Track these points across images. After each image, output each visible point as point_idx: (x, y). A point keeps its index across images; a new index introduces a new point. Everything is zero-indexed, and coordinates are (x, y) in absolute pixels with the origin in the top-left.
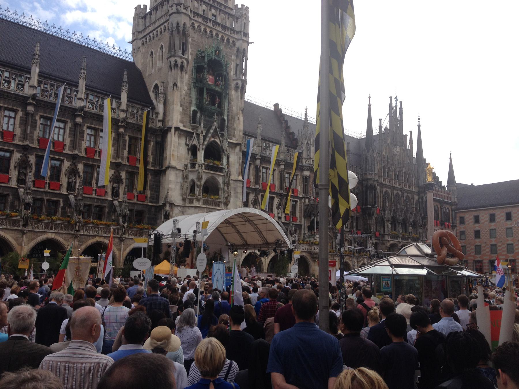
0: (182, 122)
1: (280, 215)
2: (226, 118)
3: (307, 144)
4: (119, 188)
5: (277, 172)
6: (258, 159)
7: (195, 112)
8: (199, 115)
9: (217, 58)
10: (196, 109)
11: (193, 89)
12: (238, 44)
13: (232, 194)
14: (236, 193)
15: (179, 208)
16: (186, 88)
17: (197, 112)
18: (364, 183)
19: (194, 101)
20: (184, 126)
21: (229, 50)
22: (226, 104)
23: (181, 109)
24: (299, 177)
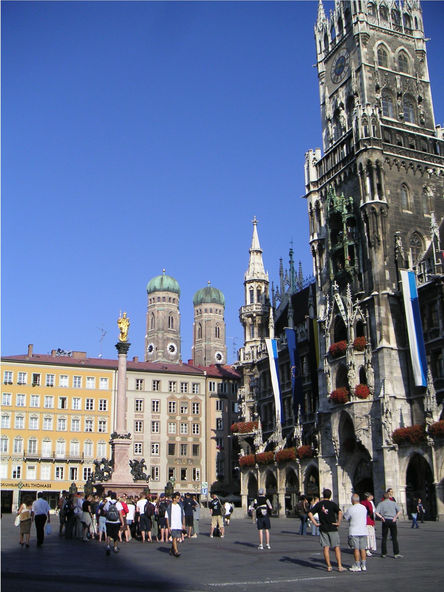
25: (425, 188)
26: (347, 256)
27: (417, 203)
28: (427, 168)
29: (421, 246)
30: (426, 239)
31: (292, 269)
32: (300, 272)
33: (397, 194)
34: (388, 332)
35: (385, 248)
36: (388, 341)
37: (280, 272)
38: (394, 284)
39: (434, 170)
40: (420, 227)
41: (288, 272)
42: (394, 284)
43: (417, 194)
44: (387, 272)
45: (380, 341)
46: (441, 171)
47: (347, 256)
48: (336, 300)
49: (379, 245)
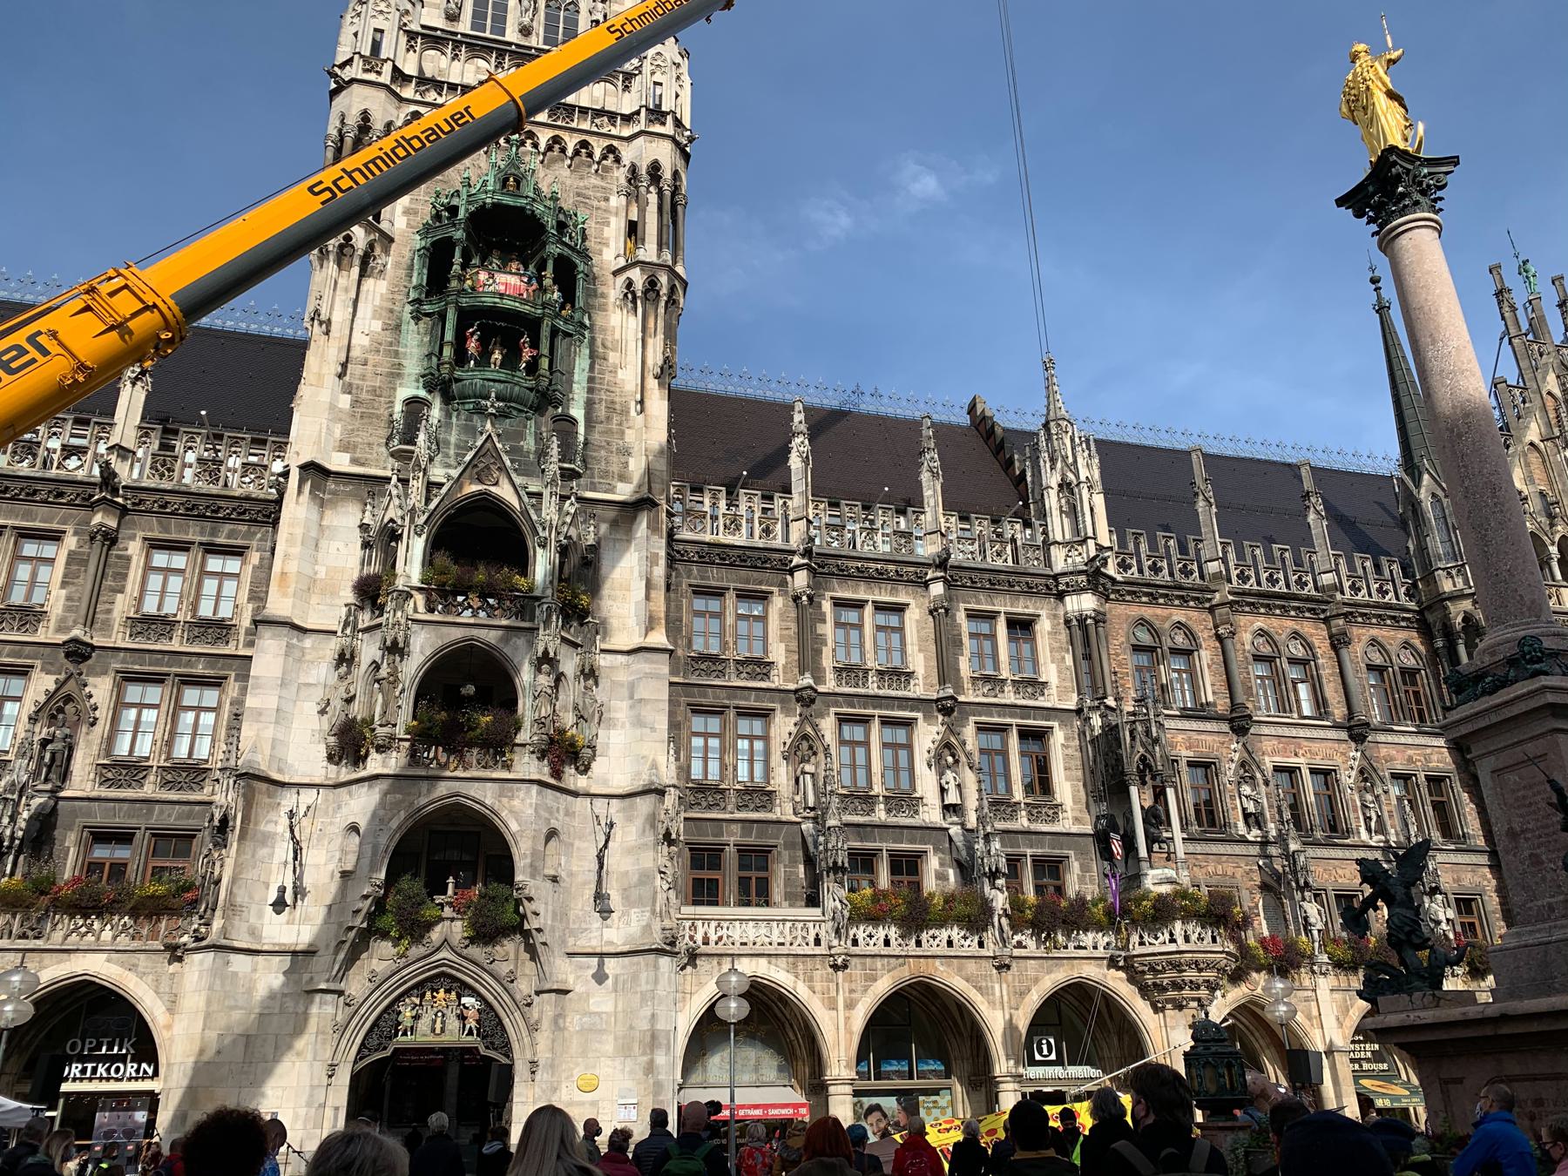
0: (345, 447)
1: (952, 798)
2: (577, 412)
3: (1065, 486)
4: (71, 749)
5: (915, 617)
6: (798, 567)
8: (436, 412)
10: (422, 393)
11: (410, 327)
12: (628, 153)
13: (620, 709)
14: (637, 703)
15: (308, 796)
16: (377, 326)
17: (428, 404)
18: (1430, 618)
19: (413, 366)
20: (354, 461)
21: (595, 181)
22: (581, 364)
23: (345, 401)
24: (1044, 626)
45: (649, 628)
48: (499, 446)
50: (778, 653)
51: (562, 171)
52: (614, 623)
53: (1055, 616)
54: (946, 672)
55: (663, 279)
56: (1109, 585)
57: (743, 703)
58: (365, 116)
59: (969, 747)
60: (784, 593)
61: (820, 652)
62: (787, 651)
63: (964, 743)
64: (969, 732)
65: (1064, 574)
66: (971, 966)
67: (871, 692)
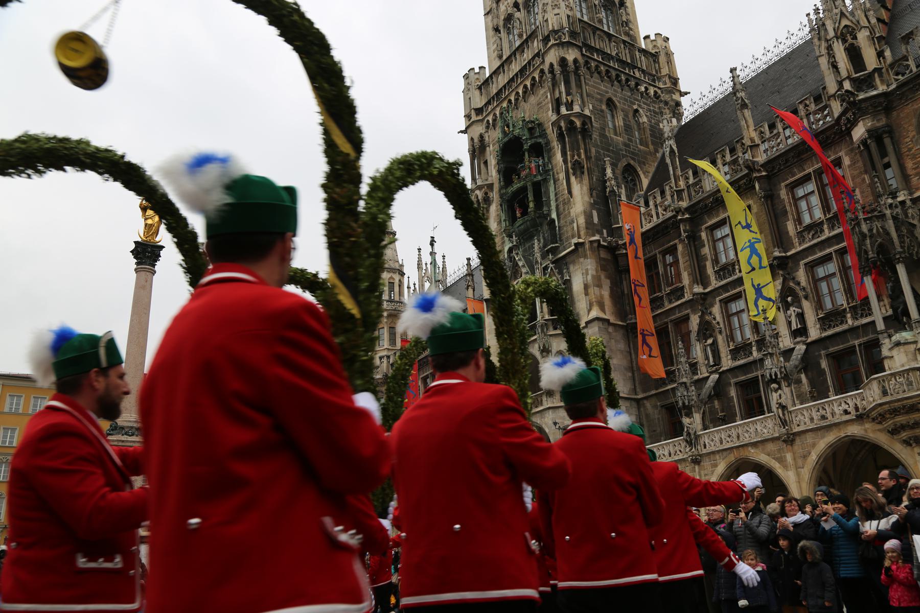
7: (510, 250)
9: (506, 139)
21: (542, 91)
22: (552, 189)
25: (636, 111)
26: (531, 198)
27: (628, 128)
28: (637, 85)
29: (635, 185)
30: (642, 176)
31: (434, 263)
32: (444, 268)
33: (602, 111)
34: (602, 296)
35: (590, 179)
36: (602, 308)
37: (418, 265)
38: (605, 231)
39: (646, 89)
40: (633, 159)
41: (429, 266)
42: (605, 231)
43: (626, 116)
44: (595, 213)
45: (589, 311)
46: (655, 92)
47: (531, 198)
49: (583, 173)
50: (686, 280)
51: (533, 100)
52: (582, 313)
53: (852, 150)
54: (779, 238)
55: (562, 124)
56: (882, 100)
57: (673, 317)
58: (472, 139)
59: (804, 283)
60: (682, 241)
61: (705, 266)
62: (689, 275)
63: (799, 284)
64: (801, 275)
65: (840, 117)
66: (771, 447)
67: (736, 277)
